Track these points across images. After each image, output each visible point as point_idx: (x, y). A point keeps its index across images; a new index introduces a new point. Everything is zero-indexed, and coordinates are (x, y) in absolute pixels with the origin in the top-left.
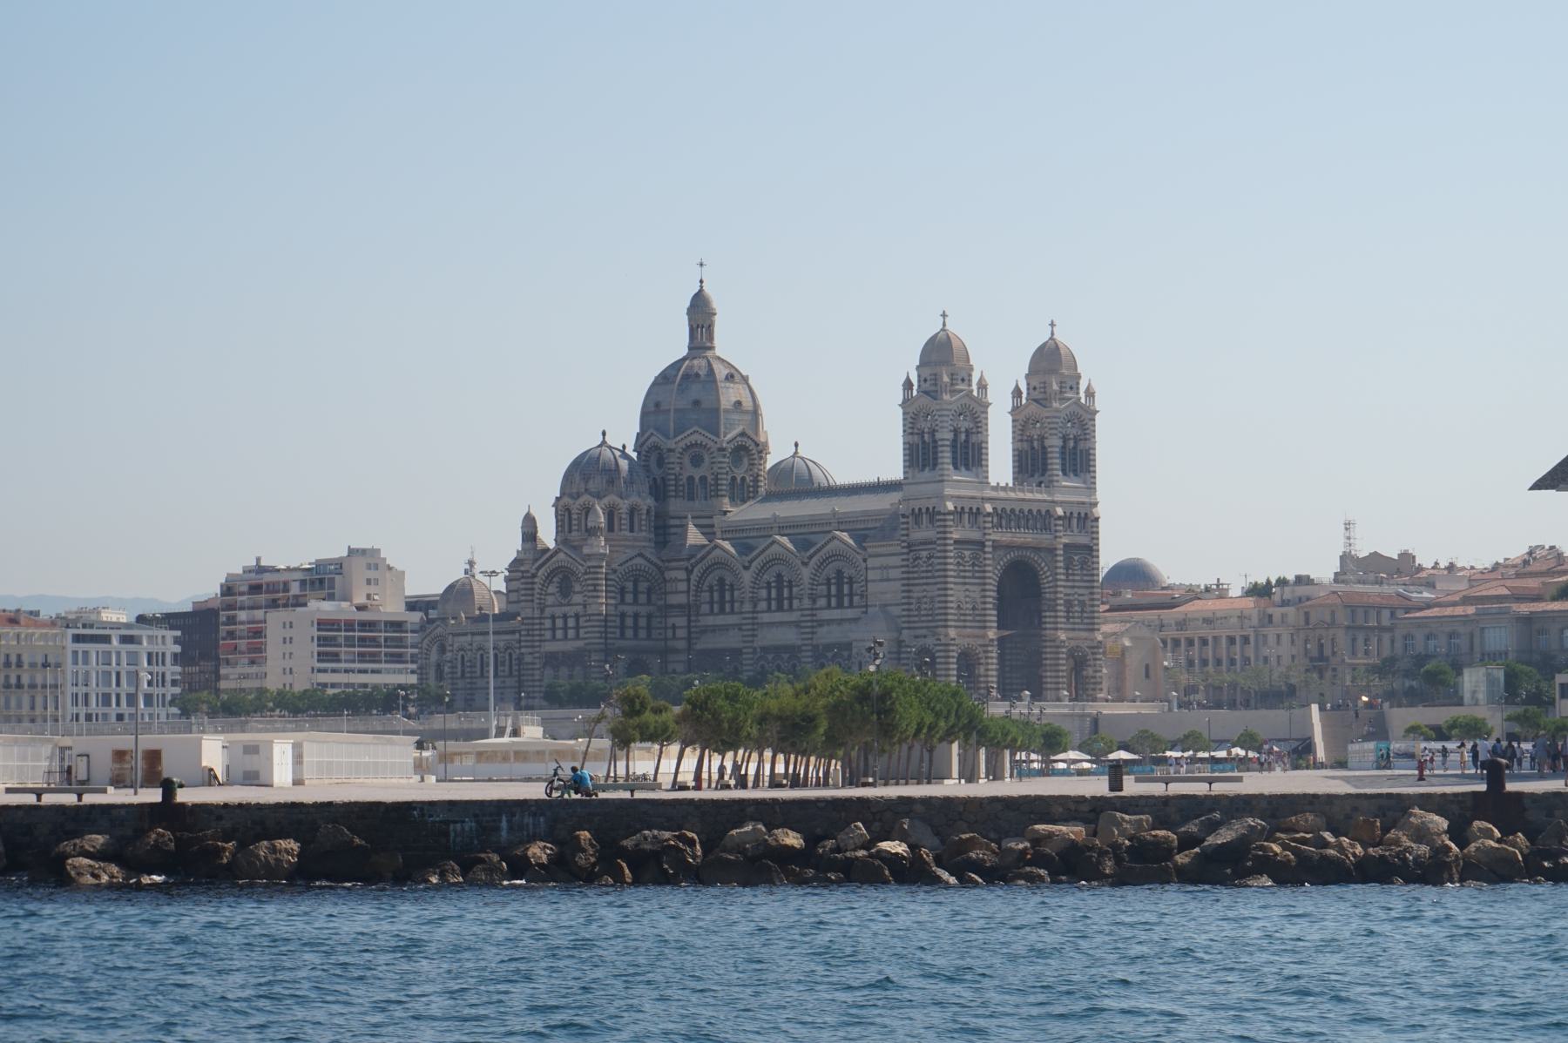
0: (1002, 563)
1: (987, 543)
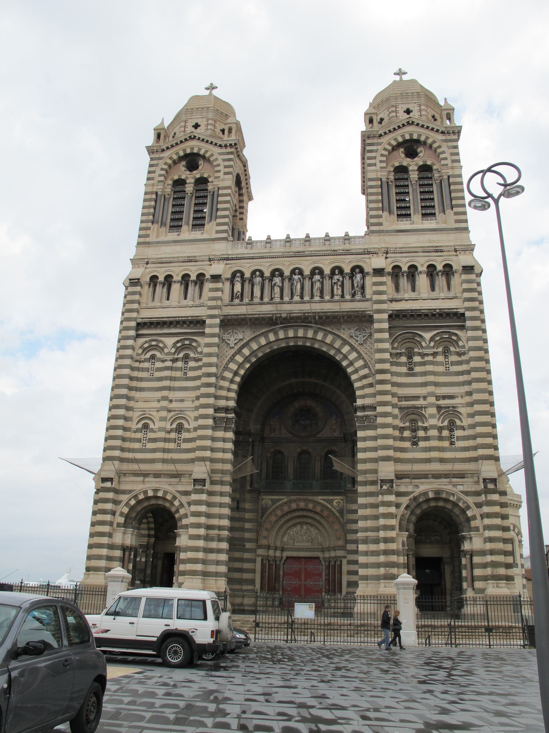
0: (246, 352)
1: (208, 321)
